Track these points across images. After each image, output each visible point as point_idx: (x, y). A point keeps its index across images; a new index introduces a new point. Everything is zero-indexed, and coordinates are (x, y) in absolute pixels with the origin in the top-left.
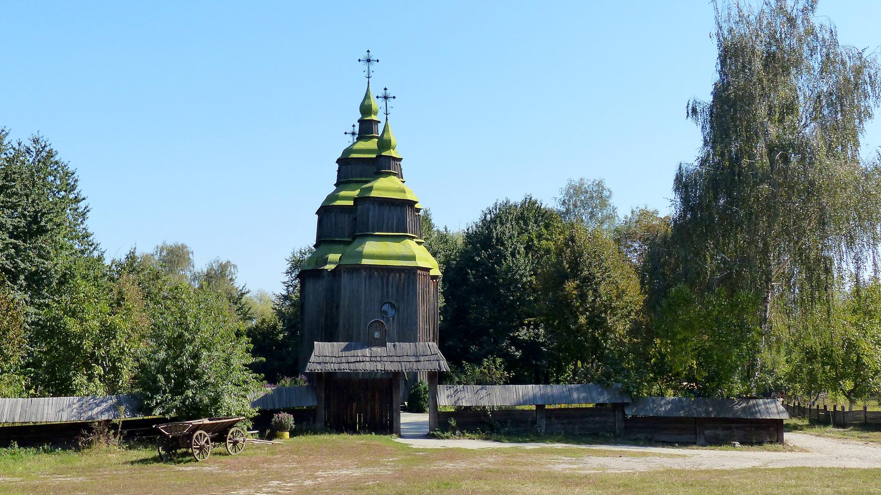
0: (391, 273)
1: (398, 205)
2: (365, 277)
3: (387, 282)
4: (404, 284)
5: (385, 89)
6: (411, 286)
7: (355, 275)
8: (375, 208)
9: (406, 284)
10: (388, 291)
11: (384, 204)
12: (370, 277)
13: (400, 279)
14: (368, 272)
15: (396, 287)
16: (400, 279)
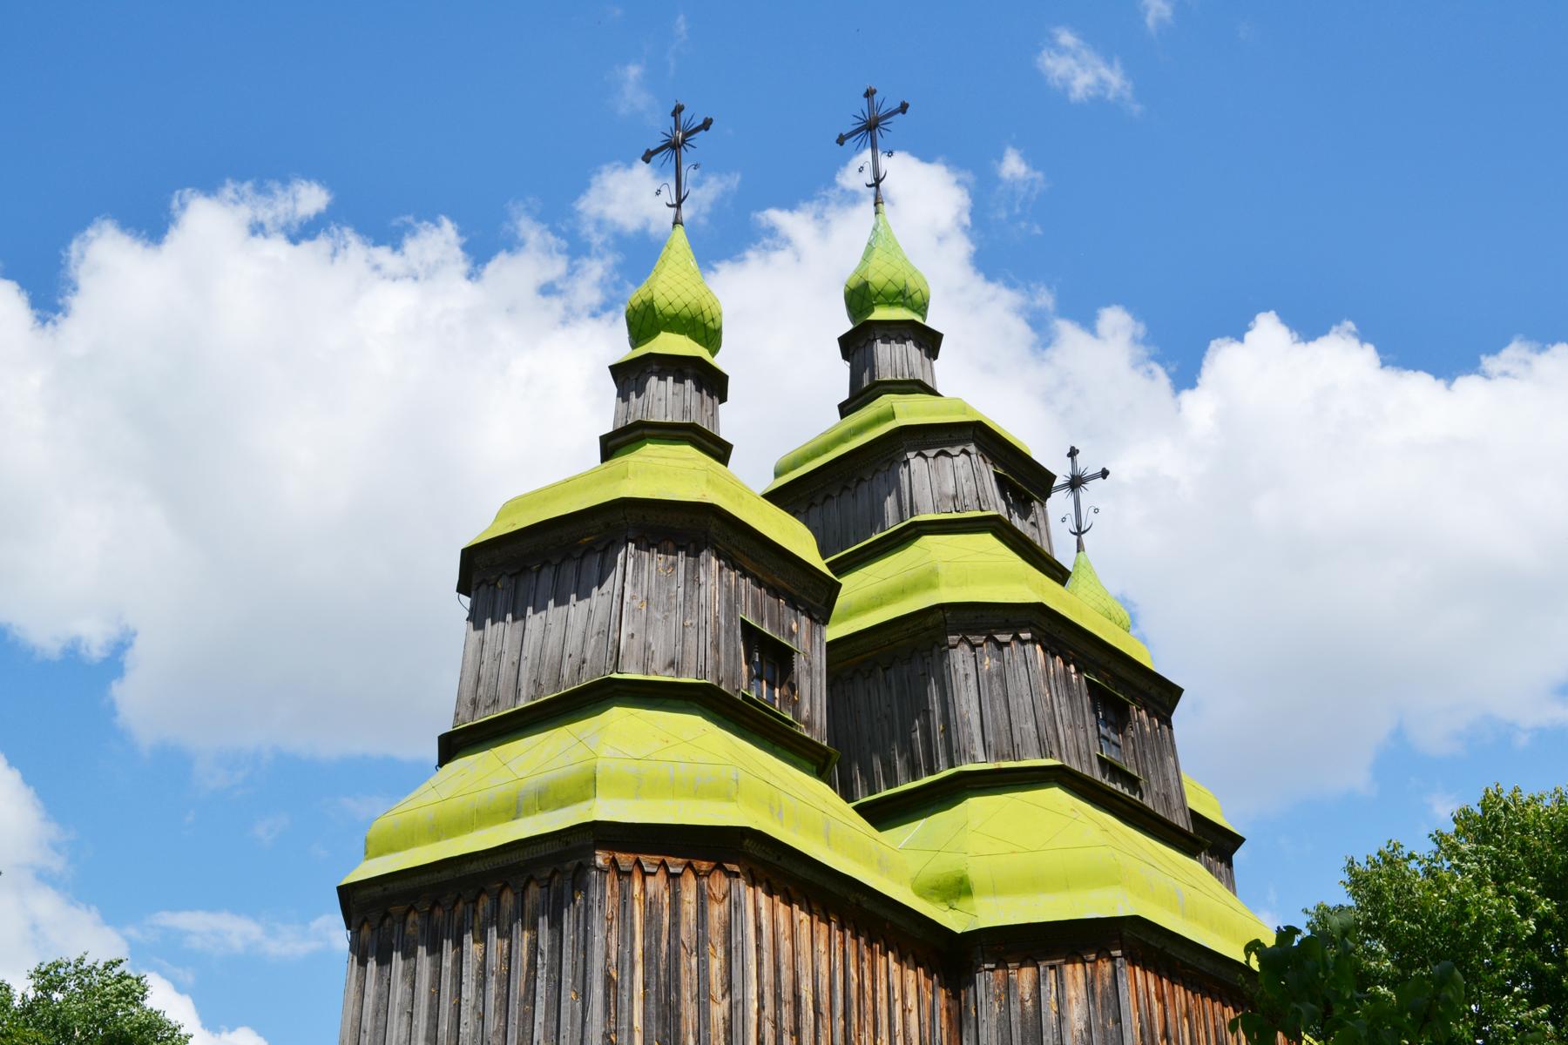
0: (476, 901)
1: (590, 549)
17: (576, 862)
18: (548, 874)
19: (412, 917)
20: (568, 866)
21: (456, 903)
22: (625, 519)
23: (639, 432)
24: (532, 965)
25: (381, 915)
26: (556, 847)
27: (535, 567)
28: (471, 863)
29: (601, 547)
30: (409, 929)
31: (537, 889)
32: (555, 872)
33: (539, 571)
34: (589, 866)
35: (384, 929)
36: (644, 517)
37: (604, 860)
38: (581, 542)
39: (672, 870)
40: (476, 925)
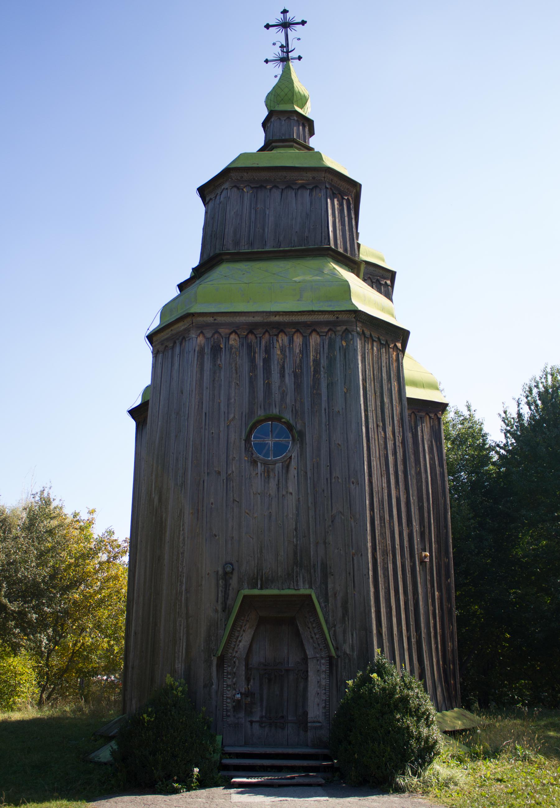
0: (277, 335)
1: (303, 187)
2: (201, 353)
3: (267, 361)
4: (317, 362)
5: (285, 12)
6: (338, 365)
7: (177, 350)
8: (242, 197)
9: (324, 362)
10: (268, 387)
11: (265, 188)
12: (216, 350)
13: (306, 344)
14: (209, 335)
15: (295, 373)
16: (306, 344)
17: (344, 327)
18: (326, 330)
19: (233, 336)
20: (339, 328)
21: (264, 334)
22: (324, 178)
23: (291, 143)
24: (317, 371)
25: (213, 332)
26: (331, 318)
27: (268, 187)
28: (275, 317)
29: (311, 187)
30: (231, 342)
31: (318, 337)
32: (330, 330)
33: (271, 189)
34: (353, 331)
35: (214, 339)
36: (332, 180)
37: (360, 329)
38: (297, 182)
39: (382, 342)
40: (278, 346)
